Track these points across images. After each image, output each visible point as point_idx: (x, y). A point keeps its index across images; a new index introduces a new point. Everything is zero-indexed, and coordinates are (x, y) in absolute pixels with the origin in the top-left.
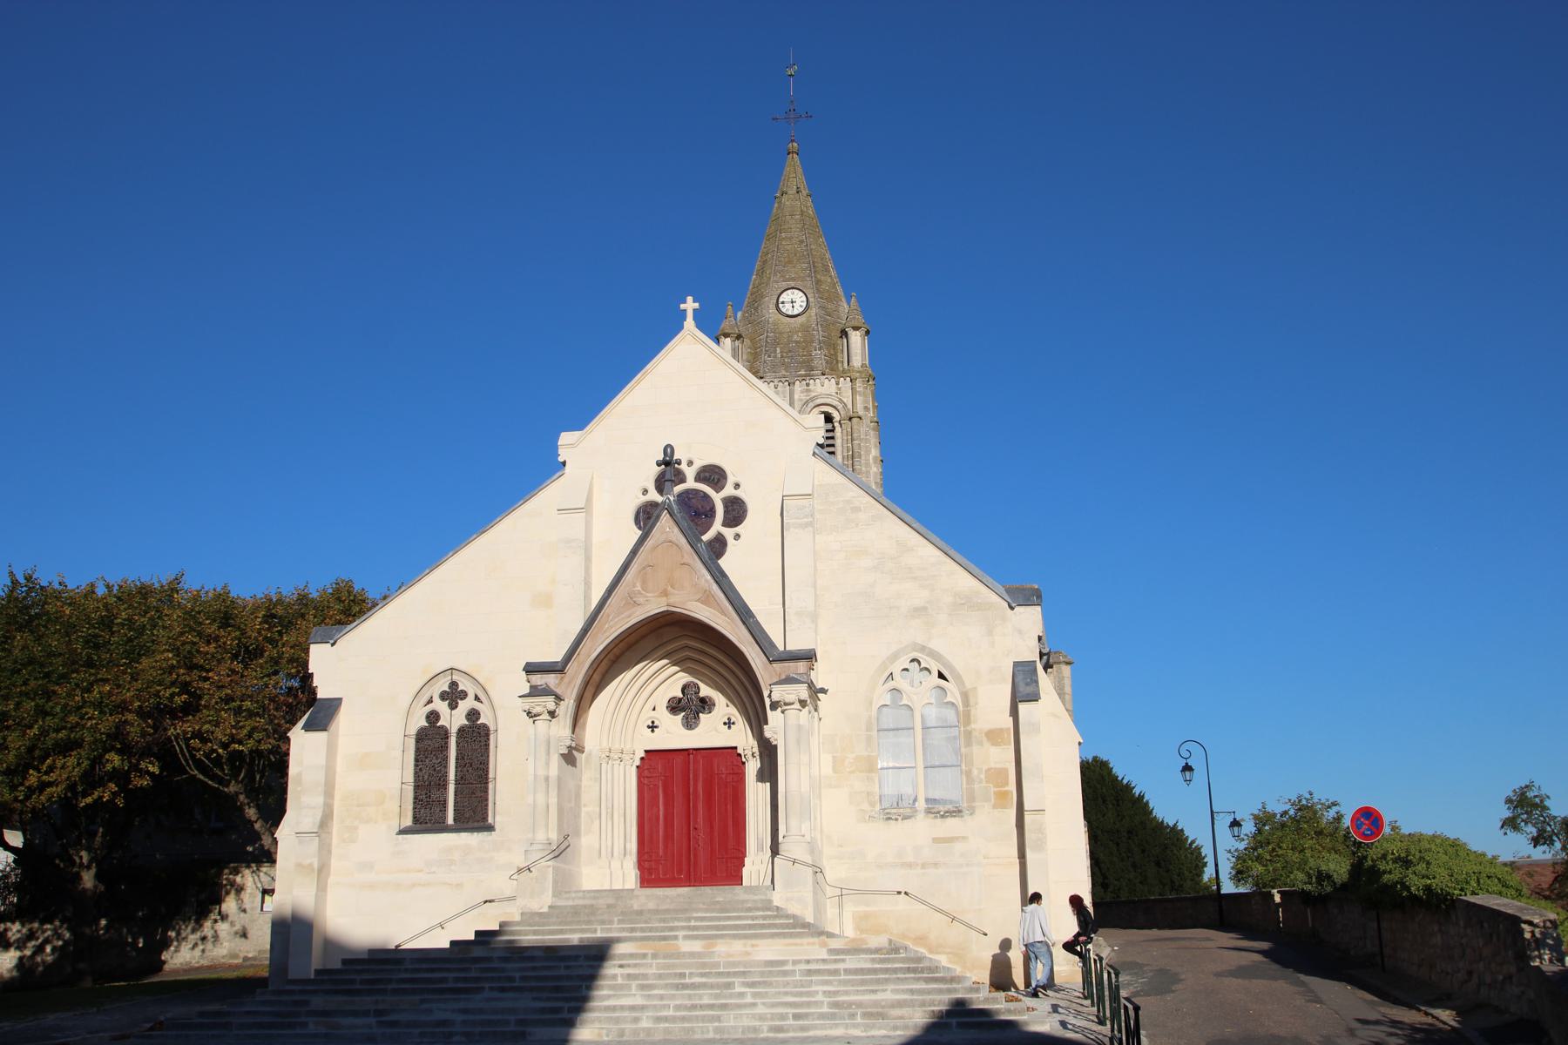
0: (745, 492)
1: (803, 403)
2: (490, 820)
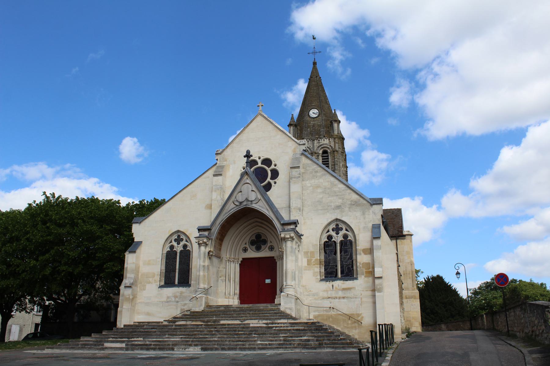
0: (278, 167)
2: (190, 283)
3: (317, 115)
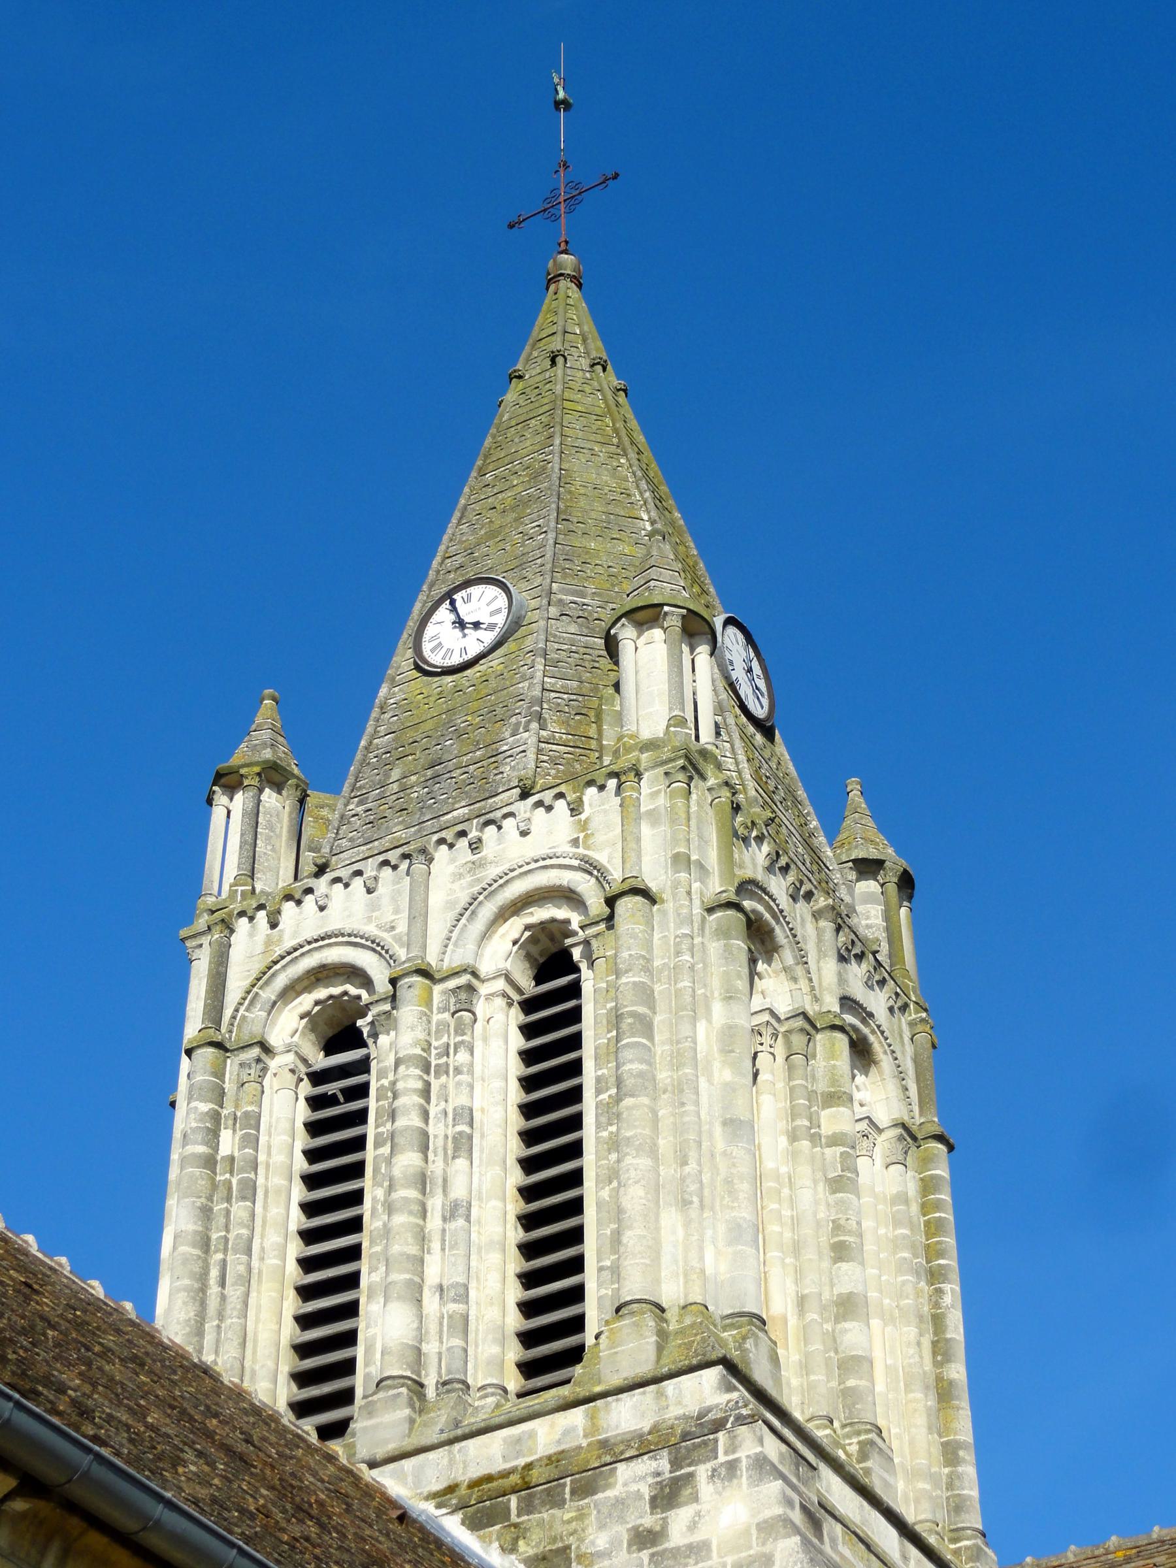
1: (459, 909)
3: (489, 637)
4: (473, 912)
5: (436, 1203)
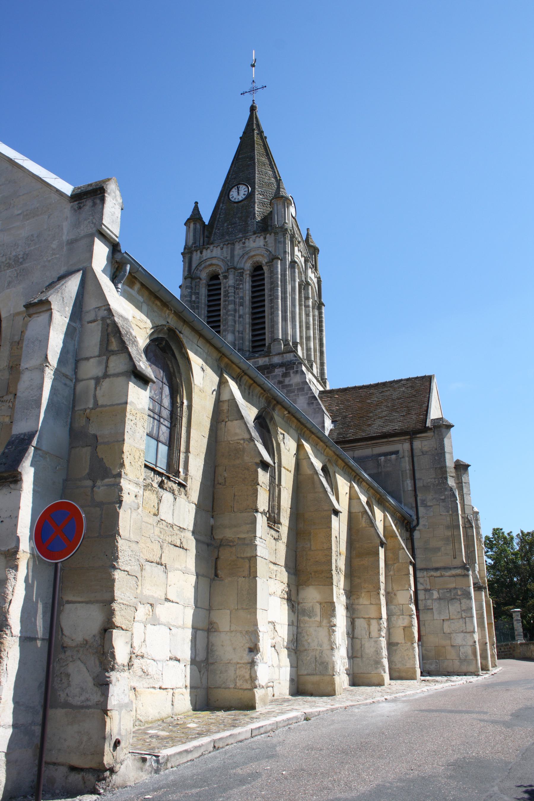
4: (243, 257)
5: (237, 315)
